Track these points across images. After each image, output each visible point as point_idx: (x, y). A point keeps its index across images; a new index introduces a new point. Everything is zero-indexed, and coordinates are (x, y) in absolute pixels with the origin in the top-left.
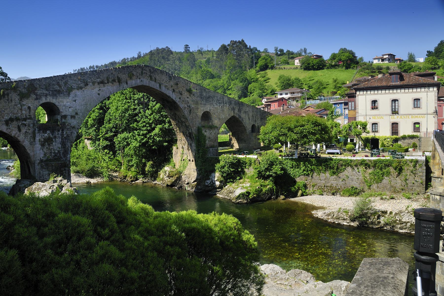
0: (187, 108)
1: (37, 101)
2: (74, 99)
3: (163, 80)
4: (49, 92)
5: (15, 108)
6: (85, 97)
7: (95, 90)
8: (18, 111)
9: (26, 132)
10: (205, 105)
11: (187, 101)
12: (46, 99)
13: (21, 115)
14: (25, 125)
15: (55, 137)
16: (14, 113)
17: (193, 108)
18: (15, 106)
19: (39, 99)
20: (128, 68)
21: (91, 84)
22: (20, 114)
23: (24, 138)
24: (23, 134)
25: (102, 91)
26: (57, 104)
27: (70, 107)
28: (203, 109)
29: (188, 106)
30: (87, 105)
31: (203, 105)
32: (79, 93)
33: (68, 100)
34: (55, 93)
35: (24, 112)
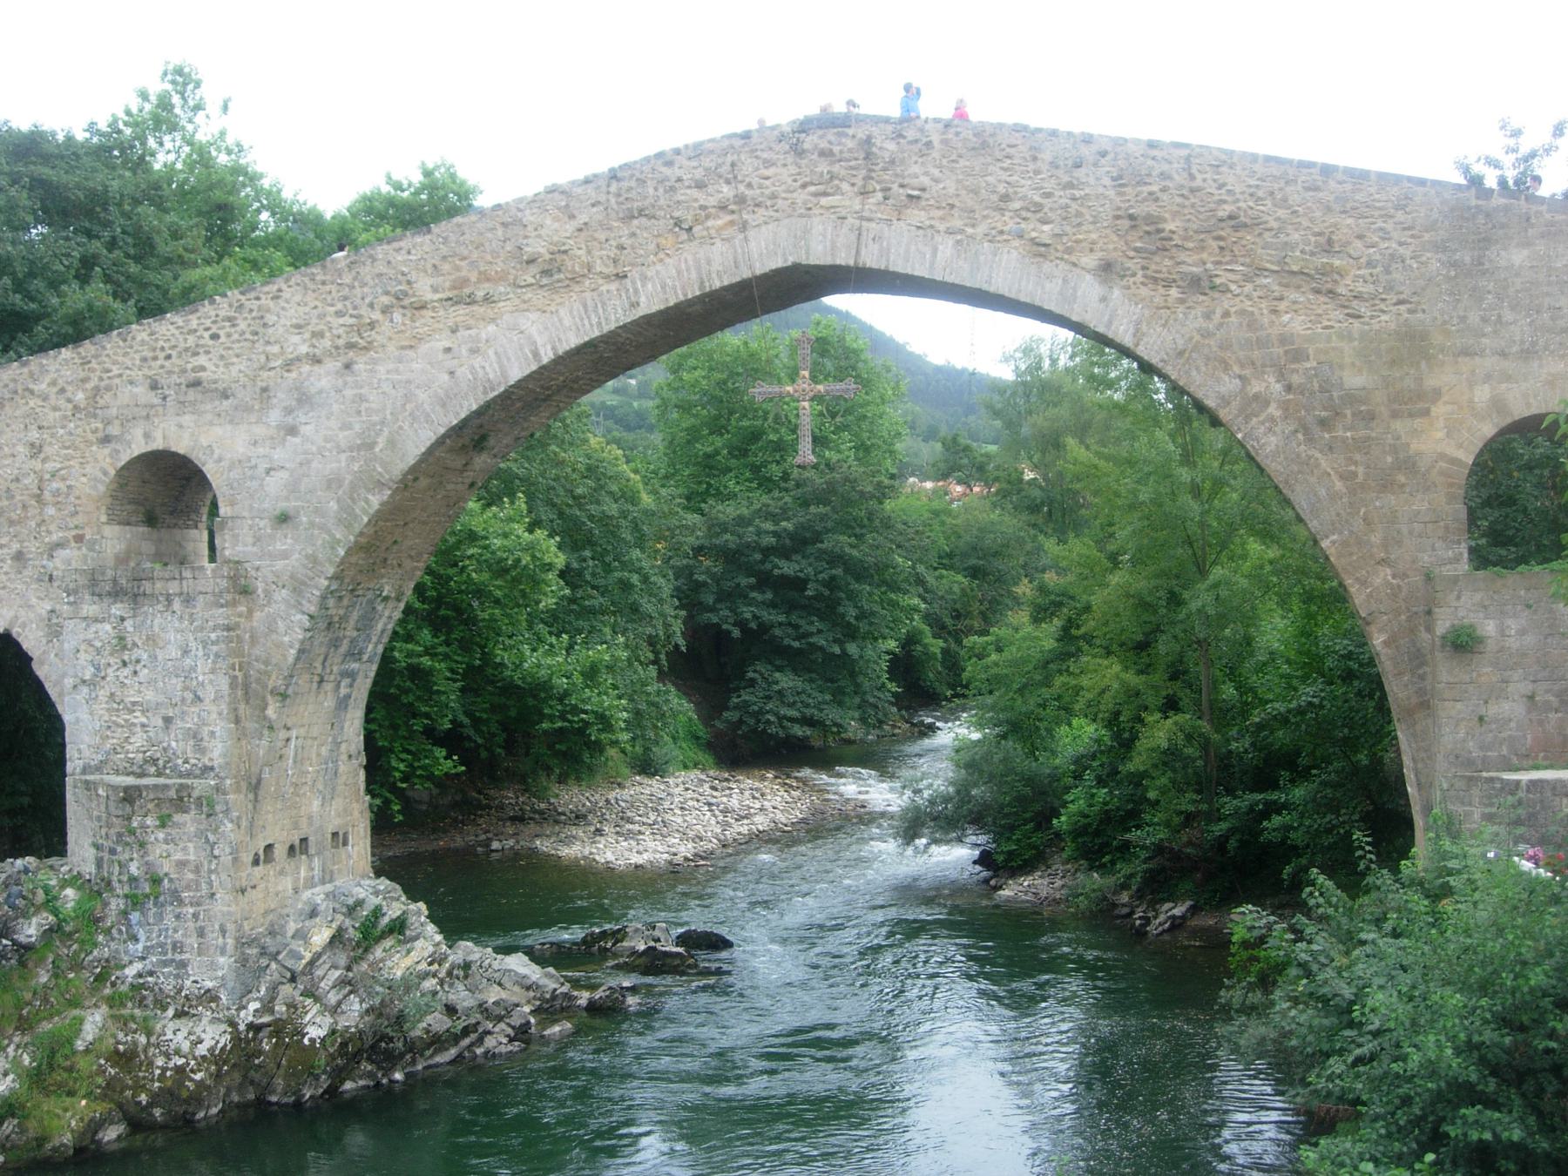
0: (1285, 406)
1: (106, 451)
2: (290, 420)
3: (1005, 198)
4: (164, 398)
5: (13, 497)
6: (362, 399)
7: (424, 348)
8: (24, 507)
9: (52, 611)
10: (1528, 354)
11: (1283, 340)
12: (147, 436)
13: (39, 525)
14: (51, 578)
15: (151, 640)
16: (11, 523)
17: (1351, 398)
18: (13, 486)
19: (118, 438)
20: (669, 164)
21: (397, 317)
22: (33, 524)
23: (44, 641)
24: (42, 620)
25: (474, 351)
26: (198, 457)
27: (268, 471)
28: (1498, 404)
29: (1289, 388)
30: (375, 443)
31: (1489, 363)
32: (322, 379)
33: (259, 431)
34: (192, 394)
35: (51, 511)
